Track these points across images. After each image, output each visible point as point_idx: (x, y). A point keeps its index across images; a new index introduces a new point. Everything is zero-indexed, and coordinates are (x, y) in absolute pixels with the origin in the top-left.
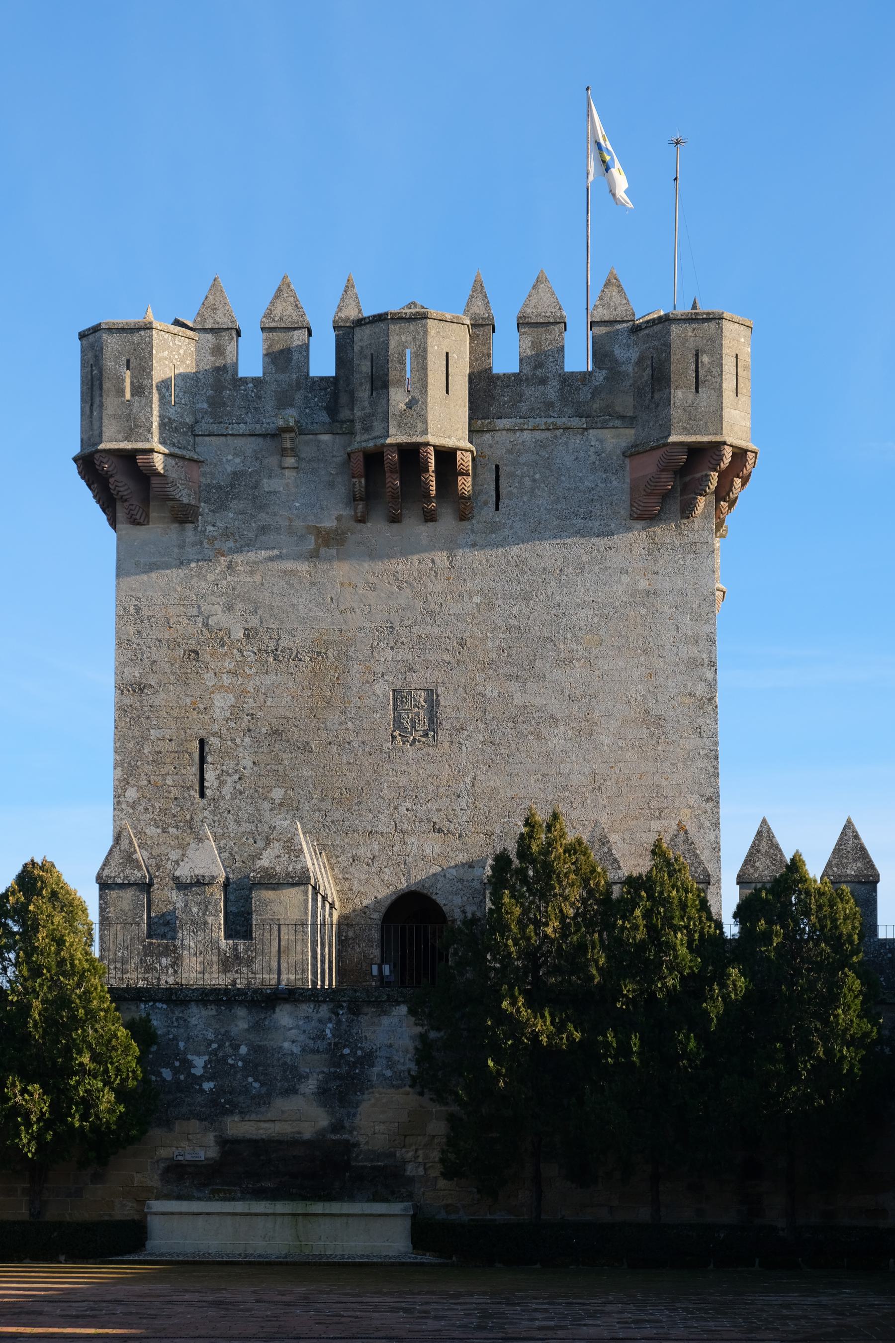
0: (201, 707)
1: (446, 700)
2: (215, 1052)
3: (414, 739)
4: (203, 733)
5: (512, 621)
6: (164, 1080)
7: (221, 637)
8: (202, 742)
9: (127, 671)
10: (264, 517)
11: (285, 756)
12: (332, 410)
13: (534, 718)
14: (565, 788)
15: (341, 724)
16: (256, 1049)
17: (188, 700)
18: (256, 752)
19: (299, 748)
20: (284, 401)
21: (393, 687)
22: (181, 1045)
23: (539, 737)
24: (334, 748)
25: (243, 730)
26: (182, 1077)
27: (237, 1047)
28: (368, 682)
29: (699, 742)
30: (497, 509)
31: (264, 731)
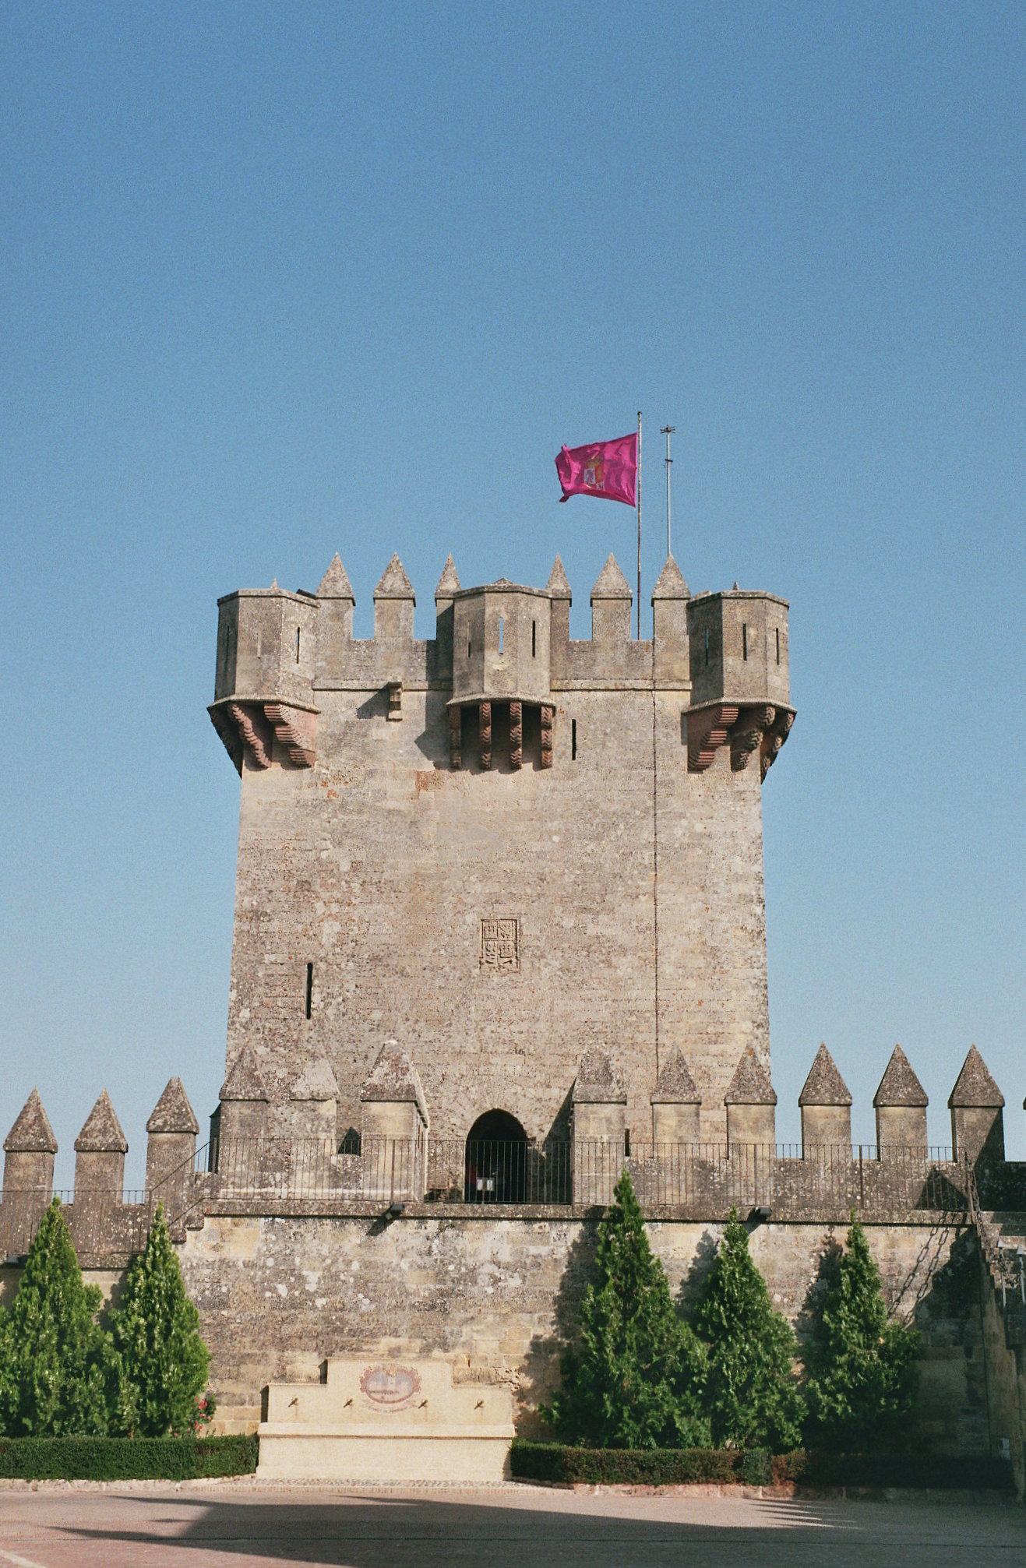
2: (328, 1268)
4: (311, 958)
5: (586, 860)
6: (279, 1297)
7: (327, 869)
8: (310, 966)
9: (246, 899)
10: (370, 765)
11: (385, 980)
14: (631, 1013)
16: (367, 1265)
17: (300, 927)
22: (297, 1261)
23: (609, 965)
26: (297, 1293)
27: (349, 1263)
29: (751, 973)
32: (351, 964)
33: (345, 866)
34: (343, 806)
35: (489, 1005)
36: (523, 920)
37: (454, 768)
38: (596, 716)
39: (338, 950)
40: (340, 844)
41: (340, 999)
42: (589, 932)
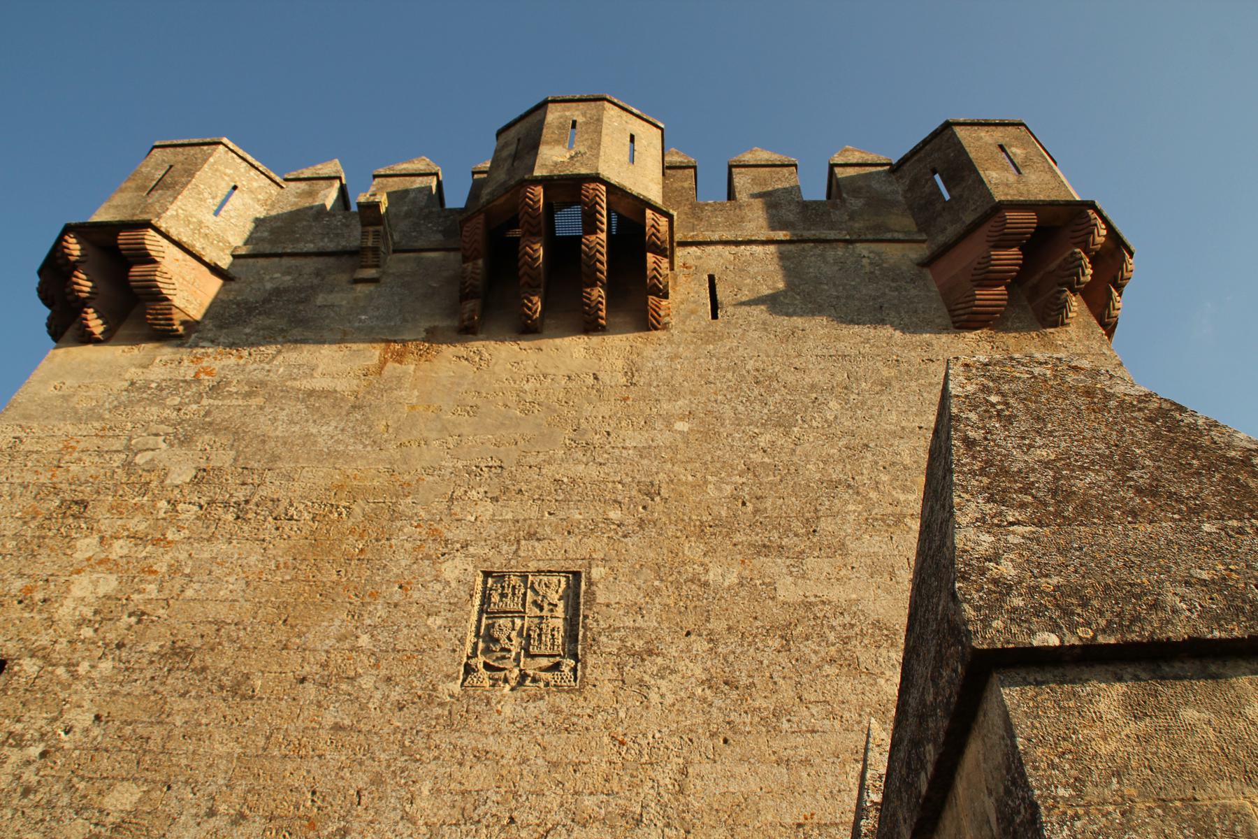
0: (39, 596)
1: (611, 593)
3: (523, 676)
13: (833, 628)
15: (341, 639)
17: (19, 584)
18: (114, 693)
19: (222, 688)
21: (486, 566)
24: (311, 689)
25: (107, 645)
28: (428, 557)
30: (715, 316)
31: (153, 647)
32: (106, 666)
33: (182, 475)
34: (215, 389)
35: (478, 776)
36: (596, 573)
37: (467, 331)
38: (752, 270)
39: (87, 632)
40: (186, 441)
41: (34, 751)
42: (782, 594)
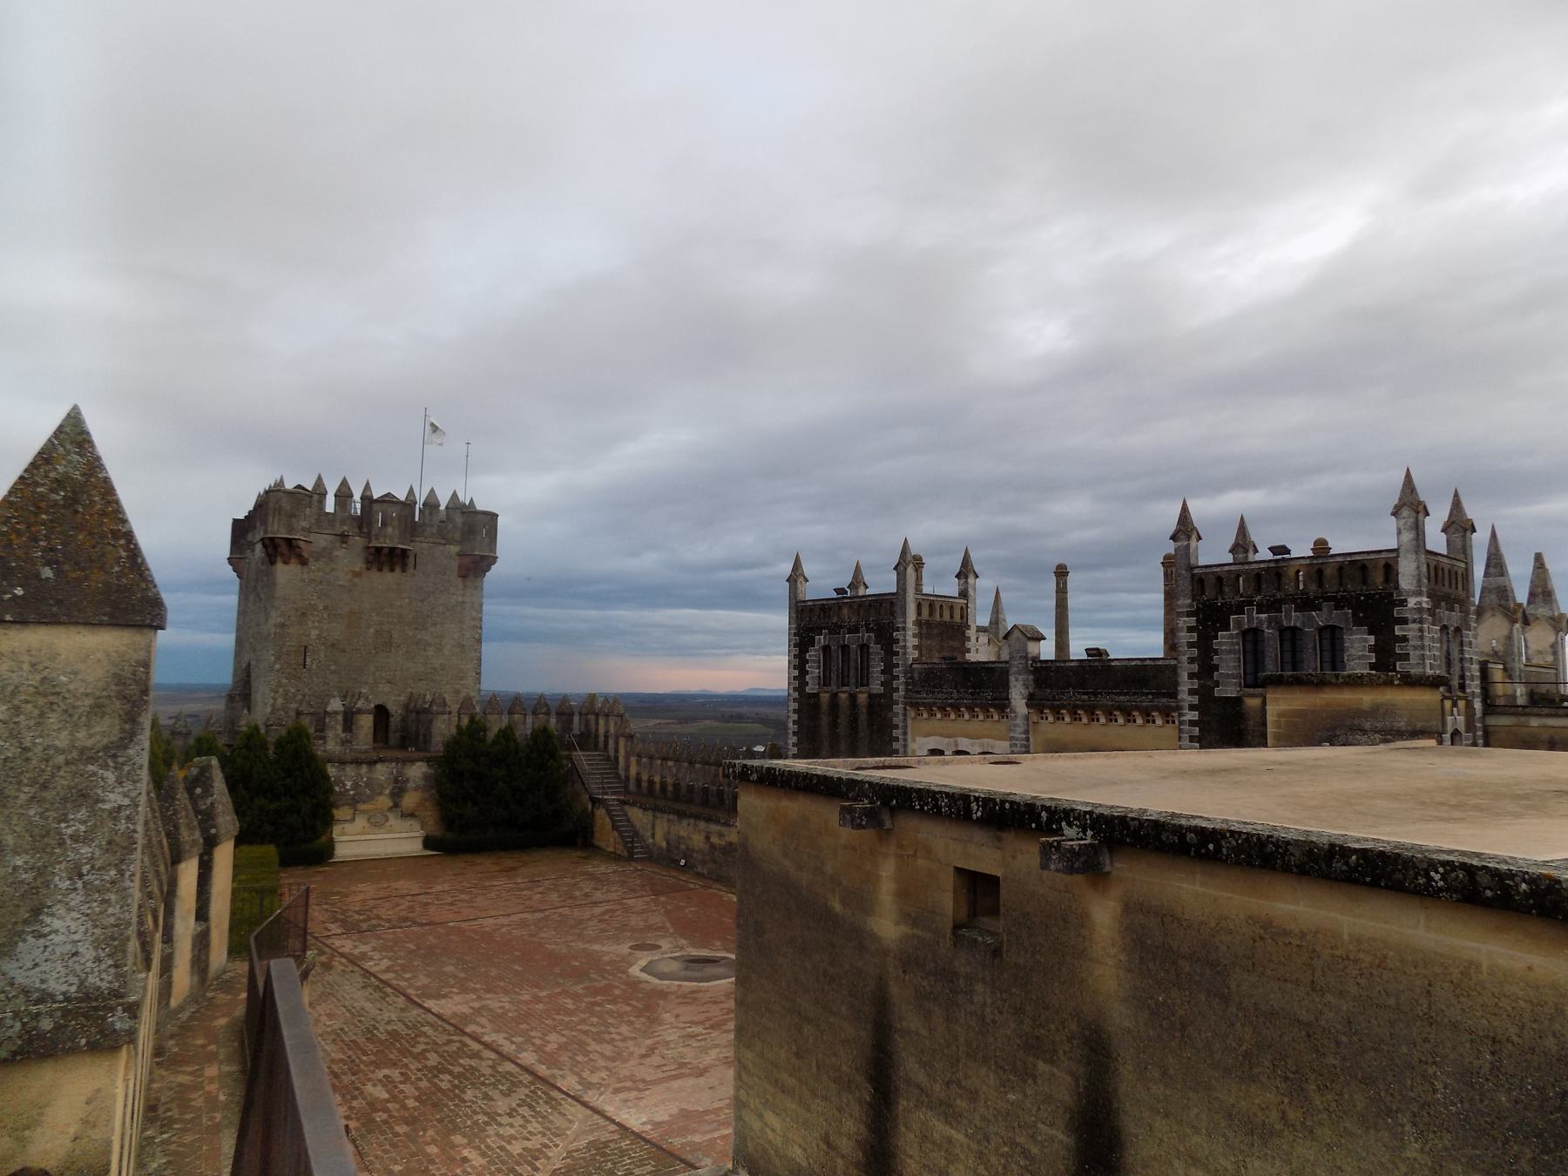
12: (360, 527)
20: (343, 523)
